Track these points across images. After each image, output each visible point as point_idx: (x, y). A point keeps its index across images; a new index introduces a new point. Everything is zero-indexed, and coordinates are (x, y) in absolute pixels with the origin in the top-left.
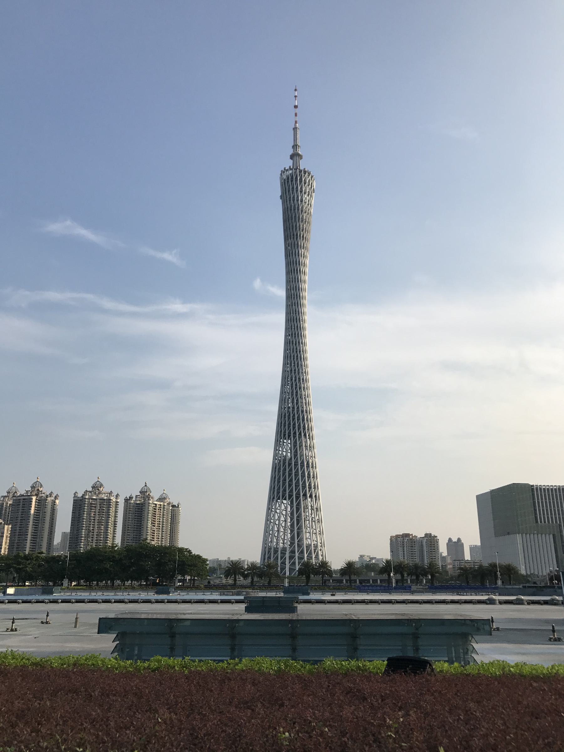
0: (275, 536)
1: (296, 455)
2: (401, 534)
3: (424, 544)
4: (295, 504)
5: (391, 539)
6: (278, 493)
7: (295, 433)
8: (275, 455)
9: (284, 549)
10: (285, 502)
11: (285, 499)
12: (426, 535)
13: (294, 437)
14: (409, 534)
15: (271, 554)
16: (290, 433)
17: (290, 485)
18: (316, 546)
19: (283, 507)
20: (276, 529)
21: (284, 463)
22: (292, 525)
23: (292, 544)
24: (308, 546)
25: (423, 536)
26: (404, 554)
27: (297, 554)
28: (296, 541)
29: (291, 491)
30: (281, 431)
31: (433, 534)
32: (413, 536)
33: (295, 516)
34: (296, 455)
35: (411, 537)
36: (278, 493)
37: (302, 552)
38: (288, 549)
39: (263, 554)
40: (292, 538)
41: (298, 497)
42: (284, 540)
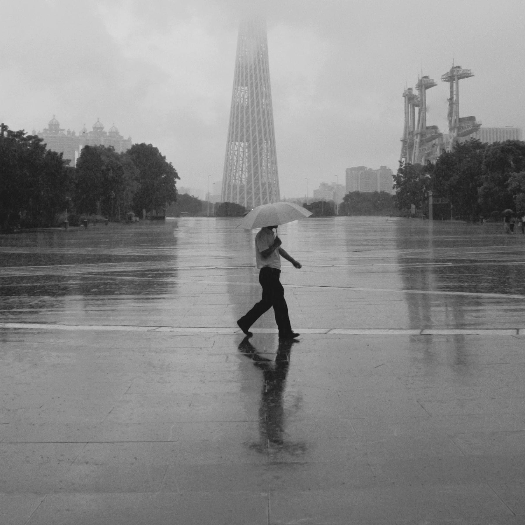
0: (235, 165)
1: (253, 104)
2: (356, 167)
3: (378, 176)
4: (252, 148)
5: (346, 172)
6: (237, 137)
7: (252, 84)
8: (234, 97)
9: (242, 187)
10: (242, 144)
11: (244, 142)
12: (382, 167)
13: (252, 87)
14: (364, 167)
15: (230, 190)
16: (247, 83)
17: (247, 131)
18: (270, 185)
19: (241, 149)
20: (235, 159)
21: (242, 111)
22: (249, 166)
23: (249, 181)
24: (263, 185)
25: (379, 168)
26: (358, 186)
27: (253, 190)
28: (253, 180)
29: (248, 137)
30: (239, 81)
31: (388, 167)
32: (368, 168)
33: (252, 159)
34: (253, 104)
35: (366, 169)
36: (237, 137)
37: (258, 189)
38: (245, 186)
39: (224, 190)
40: (250, 177)
41: (254, 142)
42: (242, 168)
